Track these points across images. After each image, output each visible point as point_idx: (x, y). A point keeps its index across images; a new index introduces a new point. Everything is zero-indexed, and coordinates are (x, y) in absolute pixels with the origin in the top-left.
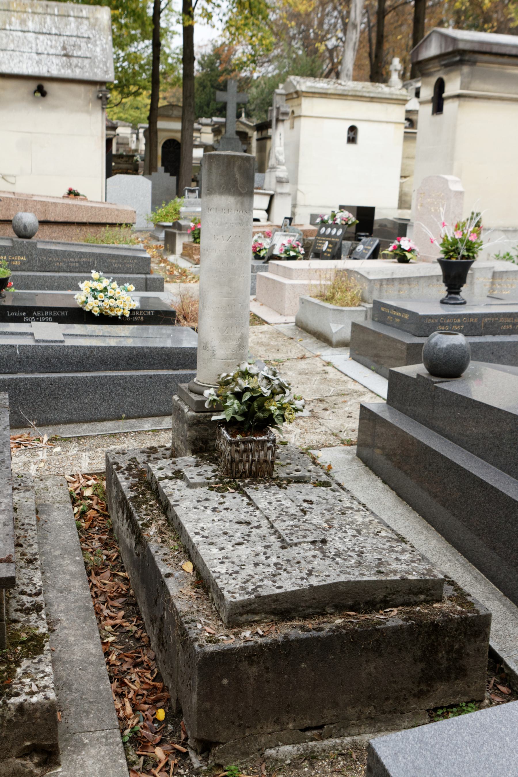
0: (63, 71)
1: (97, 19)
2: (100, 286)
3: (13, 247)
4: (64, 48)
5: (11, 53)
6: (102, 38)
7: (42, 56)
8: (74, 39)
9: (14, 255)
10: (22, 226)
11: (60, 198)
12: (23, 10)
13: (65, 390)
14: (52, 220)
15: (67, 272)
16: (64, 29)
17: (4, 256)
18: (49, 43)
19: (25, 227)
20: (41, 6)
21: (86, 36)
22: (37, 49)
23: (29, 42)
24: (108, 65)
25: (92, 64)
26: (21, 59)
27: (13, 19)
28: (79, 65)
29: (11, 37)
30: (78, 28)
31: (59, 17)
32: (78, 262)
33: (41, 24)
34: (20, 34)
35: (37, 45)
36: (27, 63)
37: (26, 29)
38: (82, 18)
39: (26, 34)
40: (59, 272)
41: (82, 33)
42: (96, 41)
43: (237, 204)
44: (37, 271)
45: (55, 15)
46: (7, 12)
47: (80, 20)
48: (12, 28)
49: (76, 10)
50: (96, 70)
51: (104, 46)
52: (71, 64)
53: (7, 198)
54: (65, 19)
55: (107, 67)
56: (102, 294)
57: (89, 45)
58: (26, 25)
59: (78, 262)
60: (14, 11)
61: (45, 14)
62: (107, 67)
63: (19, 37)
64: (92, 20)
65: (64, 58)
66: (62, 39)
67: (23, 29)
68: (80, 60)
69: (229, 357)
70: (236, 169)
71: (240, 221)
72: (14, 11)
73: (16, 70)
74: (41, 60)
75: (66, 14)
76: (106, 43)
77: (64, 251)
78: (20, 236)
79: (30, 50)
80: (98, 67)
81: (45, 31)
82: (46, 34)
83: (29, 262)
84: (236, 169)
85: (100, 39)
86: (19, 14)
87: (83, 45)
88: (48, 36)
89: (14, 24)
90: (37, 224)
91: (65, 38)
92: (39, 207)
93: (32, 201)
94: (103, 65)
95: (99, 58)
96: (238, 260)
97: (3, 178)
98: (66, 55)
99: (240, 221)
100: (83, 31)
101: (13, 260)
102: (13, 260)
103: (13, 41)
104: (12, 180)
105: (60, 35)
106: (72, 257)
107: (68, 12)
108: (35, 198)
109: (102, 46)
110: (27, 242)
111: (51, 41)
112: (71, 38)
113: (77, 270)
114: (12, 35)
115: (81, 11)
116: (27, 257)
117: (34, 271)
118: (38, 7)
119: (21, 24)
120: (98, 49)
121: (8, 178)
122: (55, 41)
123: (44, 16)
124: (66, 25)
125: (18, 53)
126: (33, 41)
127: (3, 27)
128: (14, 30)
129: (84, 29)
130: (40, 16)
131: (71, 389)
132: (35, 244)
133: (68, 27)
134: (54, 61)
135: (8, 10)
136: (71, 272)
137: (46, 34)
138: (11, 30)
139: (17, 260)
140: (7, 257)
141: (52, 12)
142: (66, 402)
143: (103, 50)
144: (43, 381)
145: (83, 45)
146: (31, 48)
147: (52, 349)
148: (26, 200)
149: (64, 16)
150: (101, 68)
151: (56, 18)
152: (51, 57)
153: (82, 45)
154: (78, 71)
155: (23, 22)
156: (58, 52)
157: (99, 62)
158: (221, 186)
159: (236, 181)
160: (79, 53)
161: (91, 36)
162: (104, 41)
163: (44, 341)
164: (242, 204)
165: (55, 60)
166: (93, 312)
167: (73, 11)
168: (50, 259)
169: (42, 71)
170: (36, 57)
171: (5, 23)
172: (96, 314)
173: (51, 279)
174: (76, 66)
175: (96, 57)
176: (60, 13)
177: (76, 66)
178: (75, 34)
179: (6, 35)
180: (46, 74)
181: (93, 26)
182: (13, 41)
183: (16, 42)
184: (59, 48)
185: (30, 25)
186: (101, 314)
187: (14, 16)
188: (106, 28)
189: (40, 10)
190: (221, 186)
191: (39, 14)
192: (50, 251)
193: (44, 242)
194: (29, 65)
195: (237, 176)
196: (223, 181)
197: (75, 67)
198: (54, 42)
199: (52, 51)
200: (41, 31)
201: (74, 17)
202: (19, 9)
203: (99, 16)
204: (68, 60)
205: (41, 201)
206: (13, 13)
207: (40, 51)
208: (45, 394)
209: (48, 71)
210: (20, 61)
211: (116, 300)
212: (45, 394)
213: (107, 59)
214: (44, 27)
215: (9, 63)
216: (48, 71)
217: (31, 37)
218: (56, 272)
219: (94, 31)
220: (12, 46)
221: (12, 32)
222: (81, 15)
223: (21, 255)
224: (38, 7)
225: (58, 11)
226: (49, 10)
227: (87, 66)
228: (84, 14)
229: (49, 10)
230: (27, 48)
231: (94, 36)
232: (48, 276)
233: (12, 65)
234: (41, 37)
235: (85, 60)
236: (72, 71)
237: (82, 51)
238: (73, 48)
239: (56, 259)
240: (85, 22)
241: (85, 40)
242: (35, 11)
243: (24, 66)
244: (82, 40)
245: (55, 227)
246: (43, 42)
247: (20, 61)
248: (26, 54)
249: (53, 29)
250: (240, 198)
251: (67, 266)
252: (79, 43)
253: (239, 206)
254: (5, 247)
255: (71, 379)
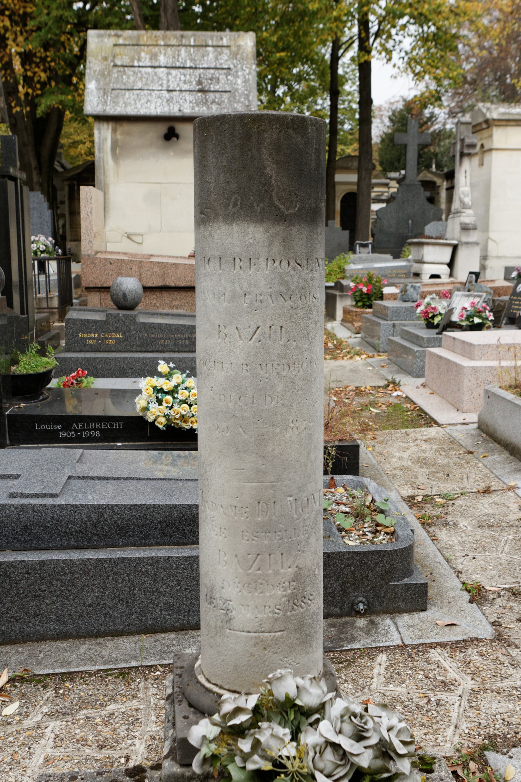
0: (197, 109)
1: (239, 47)
2: (167, 385)
3: (105, 322)
4: (200, 83)
5: (139, 92)
6: (244, 68)
7: (174, 93)
8: (212, 71)
9: (108, 332)
10: (121, 294)
11: (185, 258)
12: (154, 43)
13: (51, 583)
14: (172, 284)
15: (174, 352)
16: (200, 61)
17: (95, 333)
18: (183, 78)
19: (124, 295)
20: (176, 37)
21: (226, 66)
22: (168, 86)
23: (160, 78)
24: (251, 98)
25: (232, 99)
26: (149, 98)
27: (143, 54)
28: (217, 100)
29: (139, 74)
30: (216, 59)
31: (196, 49)
32: (189, 339)
33: (174, 57)
34: (149, 70)
35: (168, 81)
36: (156, 102)
37: (156, 64)
38: (222, 46)
39: (157, 70)
40: (164, 352)
41: (221, 64)
42: (237, 72)
43: (271, 245)
44: (137, 352)
45: (190, 46)
46: (136, 47)
47: (219, 49)
48: (141, 64)
49: (215, 38)
50: (235, 105)
51: (247, 77)
52: (207, 101)
53: (118, 260)
54: (202, 50)
55: (249, 101)
56: (169, 398)
57: (229, 77)
58: (157, 60)
59: (189, 339)
60: (144, 45)
61: (179, 46)
62: (249, 101)
63: (149, 74)
64: (233, 49)
65: (199, 94)
66: (197, 72)
67: (153, 65)
68: (218, 95)
69: (267, 626)
70: (265, 153)
71: (283, 289)
72: (144, 45)
73: (143, 111)
74: (172, 98)
75: (204, 44)
76: (249, 74)
77: (171, 325)
78: (121, 307)
79: (160, 88)
80: (239, 101)
81: (178, 64)
82: (179, 68)
83: (126, 340)
84: (265, 153)
85: (242, 69)
86: (150, 48)
87: (222, 77)
88: (181, 70)
89: (143, 60)
90: (141, 291)
91: (201, 70)
92: (156, 269)
93: (147, 263)
94: (245, 99)
95: (240, 91)
96: (280, 388)
97: (128, 237)
98: (200, 91)
99: (283, 289)
100: (222, 61)
101: (106, 338)
102: (106, 338)
103: (141, 79)
104: (138, 239)
105: (196, 68)
106: (181, 333)
107: (206, 41)
108: (153, 259)
109: (245, 77)
110: (123, 315)
111: (185, 76)
112: (208, 71)
113: (187, 349)
114: (140, 72)
115: (222, 39)
116: (124, 333)
117: (132, 351)
118: (172, 39)
119: (151, 59)
120: (239, 81)
121: (134, 238)
122: (190, 75)
123: (178, 48)
124: (203, 56)
125: (146, 92)
126: (165, 78)
127: (131, 64)
128: (142, 67)
129: (224, 60)
130: (173, 49)
131: (62, 581)
132: (134, 317)
133: (206, 58)
134: (187, 98)
135: (137, 45)
136: (179, 352)
137: (179, 68)
138: (139, 67)
139: (111, 338)
140: (99, 335)
141: (187, 43)
142: (53, 603)
143: (246, 81)
144: (14, 567)
145: (222, 77)
146: (161, 85)
147: (34, 511)
148: (141, 262)
149: (202, 46)
150: (242, 103)
151: (192, 50)
152: (184, 94)
153: (221, 77)
154: (214, 107)
155: (154, 56)
156: (192, 88)
157: (240, 96)
158: (228, 199)
159: (267, 183)
160: (217, 87)
161: (232, 66)
162: (247, 71)
163: (23, 495)
164: (286, 242)
165: (189, 97)
166: (156, 424)
167: (212, 40)
168: (153, 336)
169: (174, 110)
170: (165, 94)
171: (133, 60)
172: (161, 426)
173: (153, 361)
174: (213, 102)
175: (237, 90)
176: (197, 43)
177: (213, 102)
178: (213, 66)
179: (134, 72)
180: (178, 114)
181: (234, 55)
182: (141, 79)
183: (144, 80)
184: (194, 83)
185: (162, 60)
186: (168, 426)
187: (144, 51)
188: (250, 56)
189: (174, 42)
190: (228, 199)
191: (173, 46)
192: (152, 326)
193: (149, 313)
194: (158, 104)
195: (271, 170)
196: (233, 186)
197: (211, 104)
198: (188, 76)
199: (185, 87)
200: (174, 65)
201: (213, 46)
202: (150, 42)
203: (242, 43)
204: (204, 96)
205: (159, 263)
206: (143, 47)
207: (171, 88)
208: (18, 590)
209: (180, 110)
210: (148, 101)
211: (190, 406)
212: (18, 590)
213: (250, 92)
214: (178, 61)
215: (136, 104)
216: (180, 110)
217: (163, 72)
218: (160, 352)
219: (235, 61)
220: (139, 85)
221: (140, 69)
222: (220, 43)
223: (117, 331)
224: (172, 39)
225: (195, 41)
226: (184, 41)
227: (226, 101)
228: (225, 42)
229: (184, 41)
230: (157, 85)
231: (235, 66)
232: (149, 358)
233: (138, 105)
234: (174, 72)
235: (224, 94)
236: (208, 108)
237: (221, 85)
238: (209, 81)
239: (161, 336)
240: (226, 51)
241: (225, 71)
242: (169, 43)
243: (153, 106)
244: (220, 71)
245: (176, 293)
246: (175, 77)
247: (148, 101)
248: (156, 92)
249: (188, 62)
250: (279, 228)
251: (175, 344)
252: (217, 75)
253: (276, 249)
254: (96, 322)
255: (61, 564)
